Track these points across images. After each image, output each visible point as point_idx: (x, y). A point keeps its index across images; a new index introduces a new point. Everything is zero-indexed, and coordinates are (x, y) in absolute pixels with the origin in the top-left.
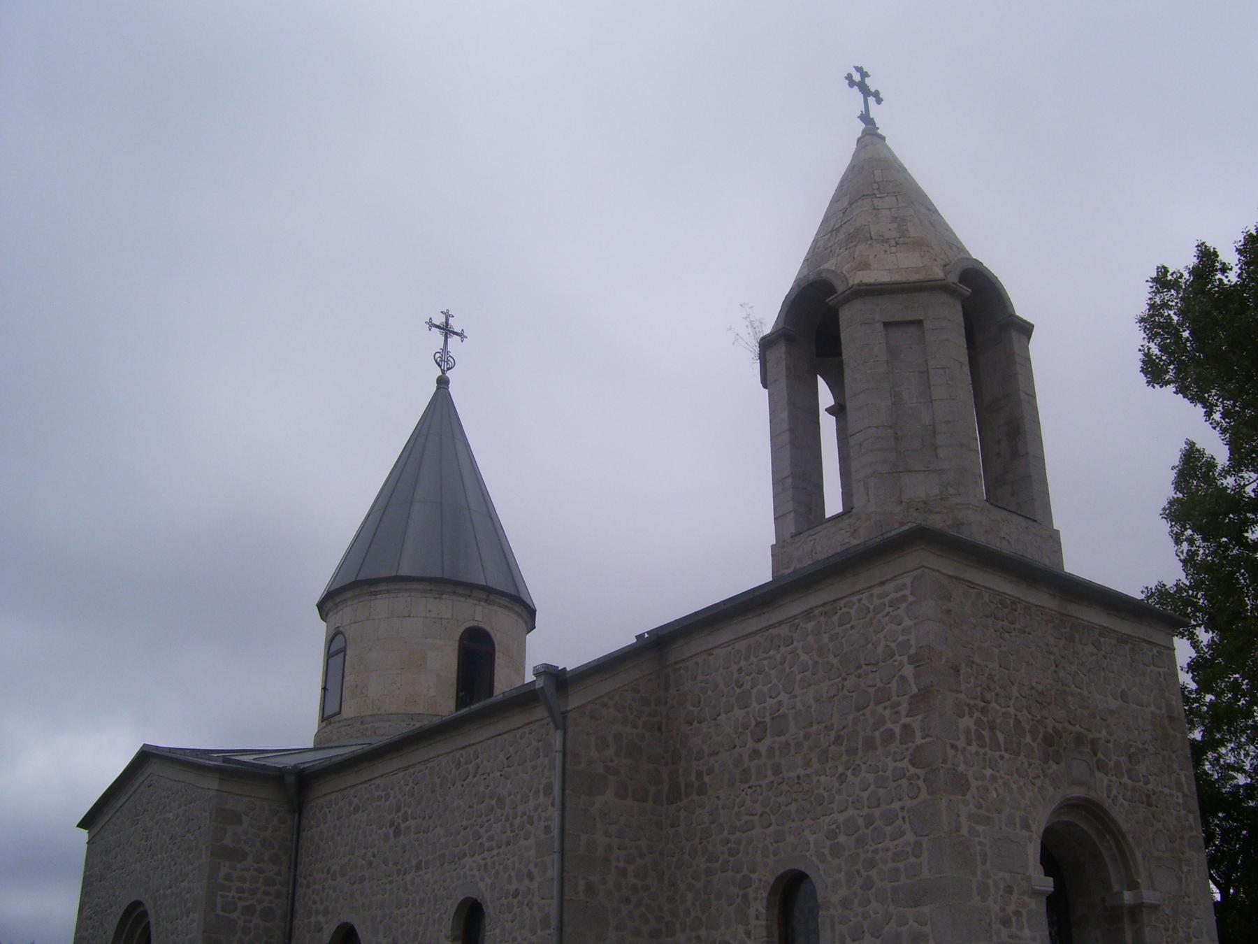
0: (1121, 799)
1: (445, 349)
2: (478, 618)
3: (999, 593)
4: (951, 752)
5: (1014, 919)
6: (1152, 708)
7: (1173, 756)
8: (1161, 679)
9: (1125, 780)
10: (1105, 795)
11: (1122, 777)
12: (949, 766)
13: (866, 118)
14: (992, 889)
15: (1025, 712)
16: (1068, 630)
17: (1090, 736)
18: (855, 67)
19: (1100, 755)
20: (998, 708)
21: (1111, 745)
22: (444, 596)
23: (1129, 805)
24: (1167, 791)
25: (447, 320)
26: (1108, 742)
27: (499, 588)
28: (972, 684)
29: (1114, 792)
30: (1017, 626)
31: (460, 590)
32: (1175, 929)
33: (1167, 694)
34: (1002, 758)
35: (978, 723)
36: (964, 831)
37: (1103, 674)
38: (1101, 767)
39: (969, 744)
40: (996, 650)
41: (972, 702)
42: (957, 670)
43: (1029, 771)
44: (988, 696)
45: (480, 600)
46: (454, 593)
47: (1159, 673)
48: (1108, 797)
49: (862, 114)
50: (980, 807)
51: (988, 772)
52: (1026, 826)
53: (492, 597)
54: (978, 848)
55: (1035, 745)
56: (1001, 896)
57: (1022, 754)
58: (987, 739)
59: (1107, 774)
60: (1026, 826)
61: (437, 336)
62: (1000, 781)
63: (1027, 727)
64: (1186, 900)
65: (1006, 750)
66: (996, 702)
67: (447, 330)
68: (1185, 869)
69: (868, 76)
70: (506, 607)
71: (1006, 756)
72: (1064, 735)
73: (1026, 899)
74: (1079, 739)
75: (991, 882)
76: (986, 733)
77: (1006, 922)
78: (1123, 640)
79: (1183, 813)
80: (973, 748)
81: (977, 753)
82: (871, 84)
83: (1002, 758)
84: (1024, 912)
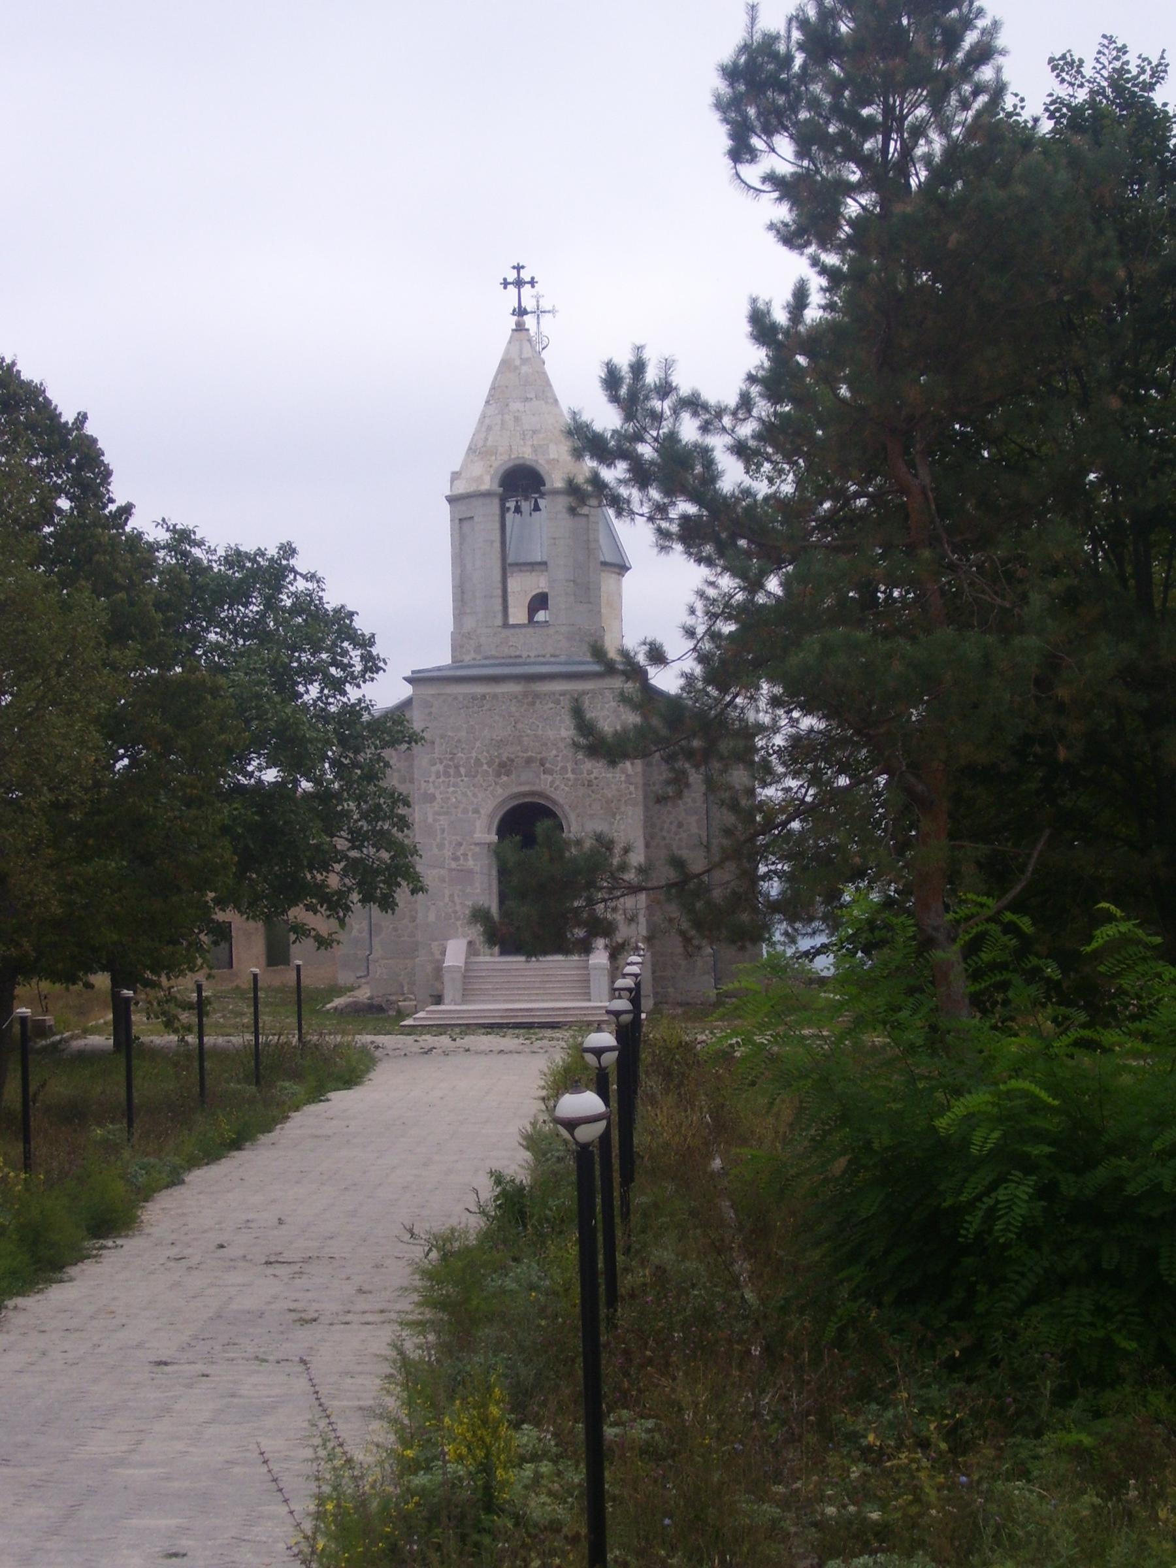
3: (470, 694)
4: (423, 785)
9: (570, 775)
11: (567, 773)
12: (422, 791)
14: (447, 845)
15: (485, 753)
16: (530, 699)
17: (539, 756)
19: (547, 765)
21: (559, 758)
25: (538, 301)
29: (557, 783)
35: (447, 766)
36: (430, 820)
37: (559, 718)
40: (465, 726)
44: (455, 751)
45: (542, 571)
49: (514, 310)
51: (452, 789)
52: (476, 811)
54: (438, 827)
55: (490, 770)
57: (479, 776)
58: (452, 774)
60: (476, 811)
63: (485, 761)
68: (618, 817)
69: (523, 267)
71: (465, 779)
73: (472, 847)
74: (529, 761)
75: (446, 842)
76: (452, 771)
77: (456, 859)
79: (623, 786)
80: (441, 780)
81: (443, 782)
82: (525, 275)
84: (470, 854)
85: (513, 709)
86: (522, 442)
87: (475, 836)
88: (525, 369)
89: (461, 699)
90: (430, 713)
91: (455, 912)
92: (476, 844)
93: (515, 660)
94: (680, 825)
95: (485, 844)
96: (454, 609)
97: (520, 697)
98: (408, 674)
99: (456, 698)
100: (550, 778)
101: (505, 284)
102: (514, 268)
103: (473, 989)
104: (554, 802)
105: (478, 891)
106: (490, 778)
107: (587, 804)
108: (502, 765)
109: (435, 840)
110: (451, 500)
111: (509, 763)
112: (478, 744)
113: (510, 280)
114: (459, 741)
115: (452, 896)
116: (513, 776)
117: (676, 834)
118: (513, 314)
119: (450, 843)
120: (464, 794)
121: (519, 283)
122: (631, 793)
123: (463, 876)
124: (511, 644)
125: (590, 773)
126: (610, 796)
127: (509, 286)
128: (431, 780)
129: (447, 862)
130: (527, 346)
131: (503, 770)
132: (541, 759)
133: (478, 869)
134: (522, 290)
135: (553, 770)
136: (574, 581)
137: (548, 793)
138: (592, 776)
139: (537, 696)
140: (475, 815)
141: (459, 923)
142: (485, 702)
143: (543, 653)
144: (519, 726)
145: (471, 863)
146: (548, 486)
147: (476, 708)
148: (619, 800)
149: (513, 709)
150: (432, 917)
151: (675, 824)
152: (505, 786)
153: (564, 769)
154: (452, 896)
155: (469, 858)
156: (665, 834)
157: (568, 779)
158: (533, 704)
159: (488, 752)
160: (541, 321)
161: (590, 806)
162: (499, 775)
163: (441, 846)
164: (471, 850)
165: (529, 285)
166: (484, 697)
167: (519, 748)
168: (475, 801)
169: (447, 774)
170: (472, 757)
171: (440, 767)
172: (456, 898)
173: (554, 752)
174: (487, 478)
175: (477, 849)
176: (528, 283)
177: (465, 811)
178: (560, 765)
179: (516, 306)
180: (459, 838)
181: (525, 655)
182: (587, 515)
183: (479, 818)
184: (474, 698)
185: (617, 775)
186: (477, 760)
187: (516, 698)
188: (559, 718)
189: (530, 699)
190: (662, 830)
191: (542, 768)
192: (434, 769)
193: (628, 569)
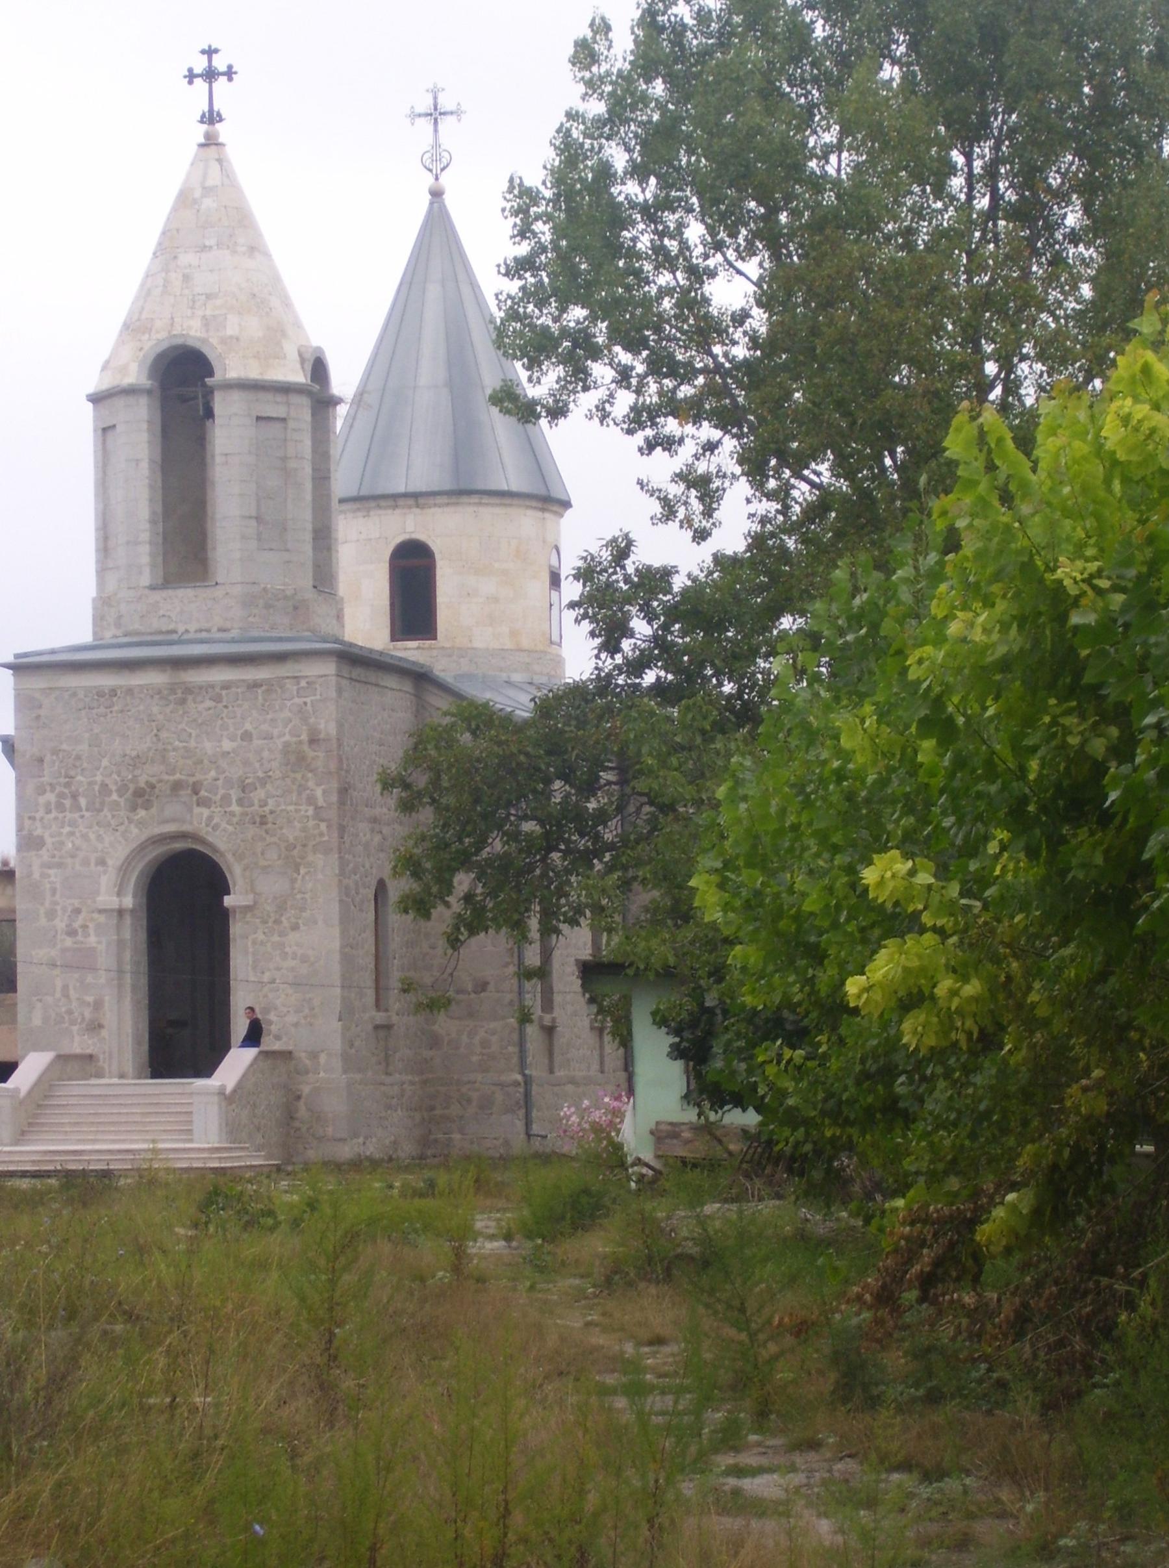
1: (436, 145)
2: (410, 527)
4: (27, 823)
5: (80, 931)
6: (287, 738)
7: (310, 775)
8: (309, 707)
9: (235, 808)
11: (230, 806)
12: (25, 832)
13: (211, 117)
14: (59, 913)
15: (115, 776)
16: (179, 695)
17: (191, 780)
19: (203, 793)
21: (220, 783)
22: (372, 513)
26: (217, 779)
27: (424, 489)
30: (116, 708)
31: (383, 503)
32: (277, 922)
33: (312, 720)
34: (82, 817)
35: (61, 795)
39: (49, 812)
41: (55, 781)
42: (41, 760)
43: (113, 822)
44: (72, 773)
45: (410, 507)
46: (379, 507)
47: (305, 703)
48: (207, 825)
49: (203, 116)
50: (53, 856)
51: (67, 829)
52: (102, 862)
53: (421, 501)
54: (48, 886)
55: (122, 801)
57: (106, 810)
60: (102, 862)
61: (426, 125)
62: (78, 834)
63: (114, 788)
64: (299, 896)
65: (87, 810)
67: (436, 115)
68: (302, 871)
69: (216, 51)
70: (448, 504)
71: (87, 814)
73: (96, 915)
74: (177, 786)
75: (58, 908)
76: (68, 803)
77: (72, 933)
78: (256, 685)
79: (311, 823)
81: (56, 818)
82: (220, 63)
83: (82, 817)
84: (91, 925)
85: (155, 710)
86: (189, 312)
87: (100, 898)
88: (208, 203)
89: (81, 695)
90: (38, 717)
91: (70, 1012)
92: (100, 911)
93: (169, 637)
95: (112, 910)
96: (97, 562)
97: (166, 692)
98: (10, 659)
100: (206, 812)
101: (191, 76)
102: (203, 52)
103: (43, 1124)
104: (215, 850)
105: (103, 981)
106: (122, 813)
107: (259, 850)
108: (139, 793)
109: (42, 904)
110: (96, 399)
112: (105, 762)
113: (198, 70)
114: (78, 758)
115: (65, 988)
116: (154, 810)
118: (202, 122)
119: (64, 909)
120: (85, 837)
121: (210, 75)
122: (321, 834)
123: (82, 962)
124: (161, 612)
125: (264, 804)
126: (291, 839)
127: (195, 80)
128: (38, 816)
129: (59, 937)
130: (215, 167)
131: (140, 801)
132: (194, 783)
133: (102, 947)
134: (214, 85)
135: (210, 799)
136: (257, 518)
137: (203, 833)
138: (267, 809)
139: (189, 690)
140: (100, 868)
141: (75, 1028)
142: (115, 699)
143: (206, 625)
144: (164, 735)
145: (92, 940)
146: (218, 376)
147: (102, 710)
148: (304, 846)
149: (155, 710)
150: (37, 1021)
152: (141, 824)
153: (226, 799)
154: (65, 988)
155: (91, 931)
157: (232, 814)
158: (183, 702)
160: (440, 127)
161: (262, 854)
162: (134, 808)
163: (51, 915)
164: (92, 920)
165: (225, 78)
166: (113, 692)
167: (162, 768)
168: (100, 846)
169: (60, 807)
170: (95, 783)
171: (51, 797)
172: (72, 992)
173: (213, 774)
174: (134, 368)
175: (102, 918)
176: (223, 74)
178: (221, 792)
179: (206, 109)
180: (76, 903)
181: (181, 629)
182: (284, 420)
183: (105, 872)
184: (101, 694)
185: (303, 808)
186: (104, 786)
187: (159, 692)
188: (220, 722)
189: (179, 695)
191: (195, 798)
192: (42, 800)
193: (566, 504)
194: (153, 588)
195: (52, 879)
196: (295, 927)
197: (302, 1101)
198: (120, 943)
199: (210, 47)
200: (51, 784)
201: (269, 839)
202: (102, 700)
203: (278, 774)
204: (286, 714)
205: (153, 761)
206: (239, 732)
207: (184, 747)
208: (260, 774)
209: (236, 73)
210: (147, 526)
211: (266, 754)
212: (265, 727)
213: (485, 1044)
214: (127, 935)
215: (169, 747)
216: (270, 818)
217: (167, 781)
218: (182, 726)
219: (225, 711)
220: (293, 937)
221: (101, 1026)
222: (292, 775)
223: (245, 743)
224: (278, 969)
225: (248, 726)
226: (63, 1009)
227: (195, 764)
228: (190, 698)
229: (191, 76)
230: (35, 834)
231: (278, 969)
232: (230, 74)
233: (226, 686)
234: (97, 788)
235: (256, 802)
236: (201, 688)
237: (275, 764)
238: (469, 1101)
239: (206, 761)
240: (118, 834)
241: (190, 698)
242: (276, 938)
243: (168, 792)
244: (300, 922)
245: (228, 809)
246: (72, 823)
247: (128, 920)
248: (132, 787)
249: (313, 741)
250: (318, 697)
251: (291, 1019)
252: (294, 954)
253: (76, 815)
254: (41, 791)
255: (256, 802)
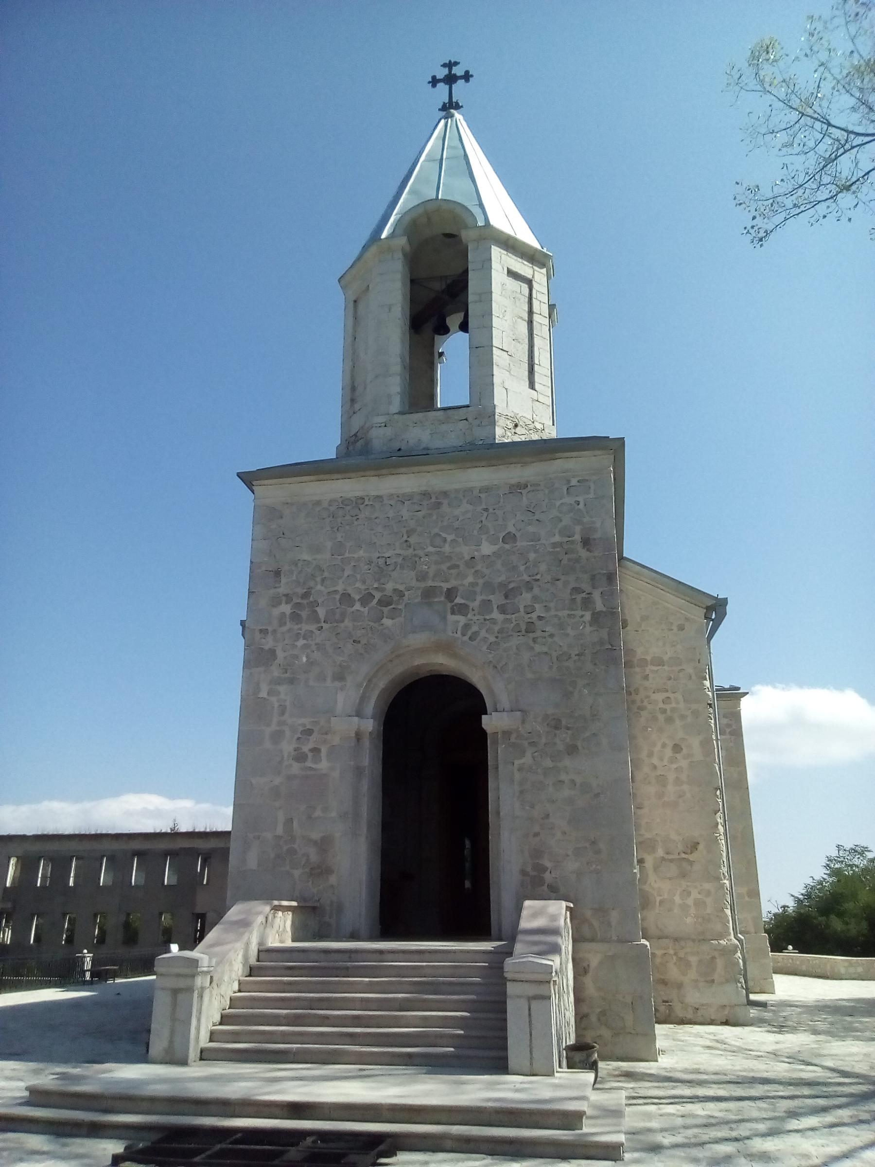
0: (483, 633)
4: (258, 635)
6: (557, 538)
8: (581, 506)
9: (496, 615)
10: (459, 632)
11: (492, 611)
14: (288, 733)
15: (358, 585)
17: (445, 586)
18: (442, 66)
19: (458, 600)
20: (323, 588)
21: (478, 589)
23: (497, 637)
24: (567, 612)
28: (294, 578)
29: (475, 628)
36: (263, 694)
38: (462, 610)
39: (282, 623)
44: (312, 584)
48: (464, 635)
49: (444, 104)
54: (276, 705)
56: (298, 739)
57: (346, 621)
59: (465, 615)
63: (357, 597)
66: (322, 585)
69: (456, 64)
71: (325, 626)
72: (407, 593)
74: (428, 594)
77: (300, 757)
79: (588, 629)
80: (285, 629)
81: (289, 630)
82: (458, 71)
84: (324, 751)
89: (325, 504)
91: (292, 852)
94: (677, 748)
99: (318, 503)
100: (462, 620)
101: (434, 82)
102: (444, 65)
105: (333, 814)
108: (385, 602)
111: (395, 598)
115: (289, 821)
117: (672, 760)
128: (270, 629)
131: (386, 610)
133: (336, 774)
135: (466, 606)
140: (338, 684)
141: (297, 873)
142: (362, 507)
145: (324, 765)
147: (348, 517)
149: (405, 513)
150: (252, 861)
151: (670, 744)
156: (655, 761)
157: (494, 621)
158: (438, 505)
159: (364, 582)
163: (277, 736)
169: (295, 617)
170: (336, 592)
171: (286, 609)
173: (470, 579)
176: (461, 77)
177: (322, 678)
178: (479, 598)
179: (447, 101)
180: (306, 721)
182: (529, 282)
183: (342, 689)
184: (345, 502)
185: (581, 613)
190: (650, 755)
191: (449, 605)
192: (276, 612)
194: (401, 413)
195: (282, 696)
196: (572, 750)
197: (590, 974)
198: (359, 771)
199: (450, 61)
200: (287, 595)
201: (538, 648)
202: (348, 508)
203: (548, 578)
204: (554, 513)
205: (402, 567)
206: (501, 535)
207: (438, 553)
208: (526, 578)
209: (472, 76)
210: (399, 360)
211: (532, 556)
212: (531, 529)
213: (698, 904)
214: (366, 761)
215: (420, 553)
216: (538, 624)
217: (418, 588)
218: (436, 530)
219: (485, 514)
220: (567, 762)
221: (329, 871)
222: (563, 578)
223: (507, 547)
224: (553, 802)
225: (511, 528)
226: (285, 848)
227: (449, 568)
228: (445, 502)
229: (434, 82)
230: (266, 647)
231: (553, 802)
232: (467, 77)
233: (486, 489)
234: (338, 597)
235: (522, 610)
236: (457, 491)
237: (543, 567)
238: (688, 965)
239: (462, 567)
240: (359, 645)
241: (445, 502)
242: (548, 763)
243: (419, 599)
244: (579, 744)
245: (487, 617)
246: (308, 635)
247: (367, 743)
248: (378, 595)
249: (586, 542)
250: (591, 496)
251: (572, 865)
252: (573, 782)
253: (313, 627)
254: (275, 602)
255: (522, 610)
